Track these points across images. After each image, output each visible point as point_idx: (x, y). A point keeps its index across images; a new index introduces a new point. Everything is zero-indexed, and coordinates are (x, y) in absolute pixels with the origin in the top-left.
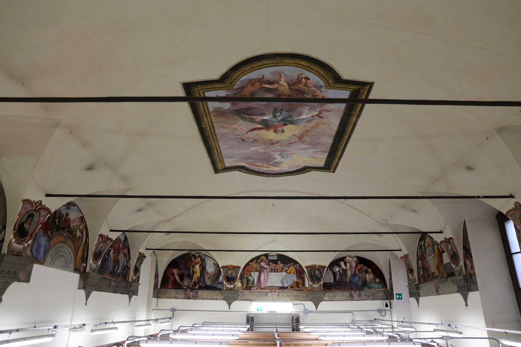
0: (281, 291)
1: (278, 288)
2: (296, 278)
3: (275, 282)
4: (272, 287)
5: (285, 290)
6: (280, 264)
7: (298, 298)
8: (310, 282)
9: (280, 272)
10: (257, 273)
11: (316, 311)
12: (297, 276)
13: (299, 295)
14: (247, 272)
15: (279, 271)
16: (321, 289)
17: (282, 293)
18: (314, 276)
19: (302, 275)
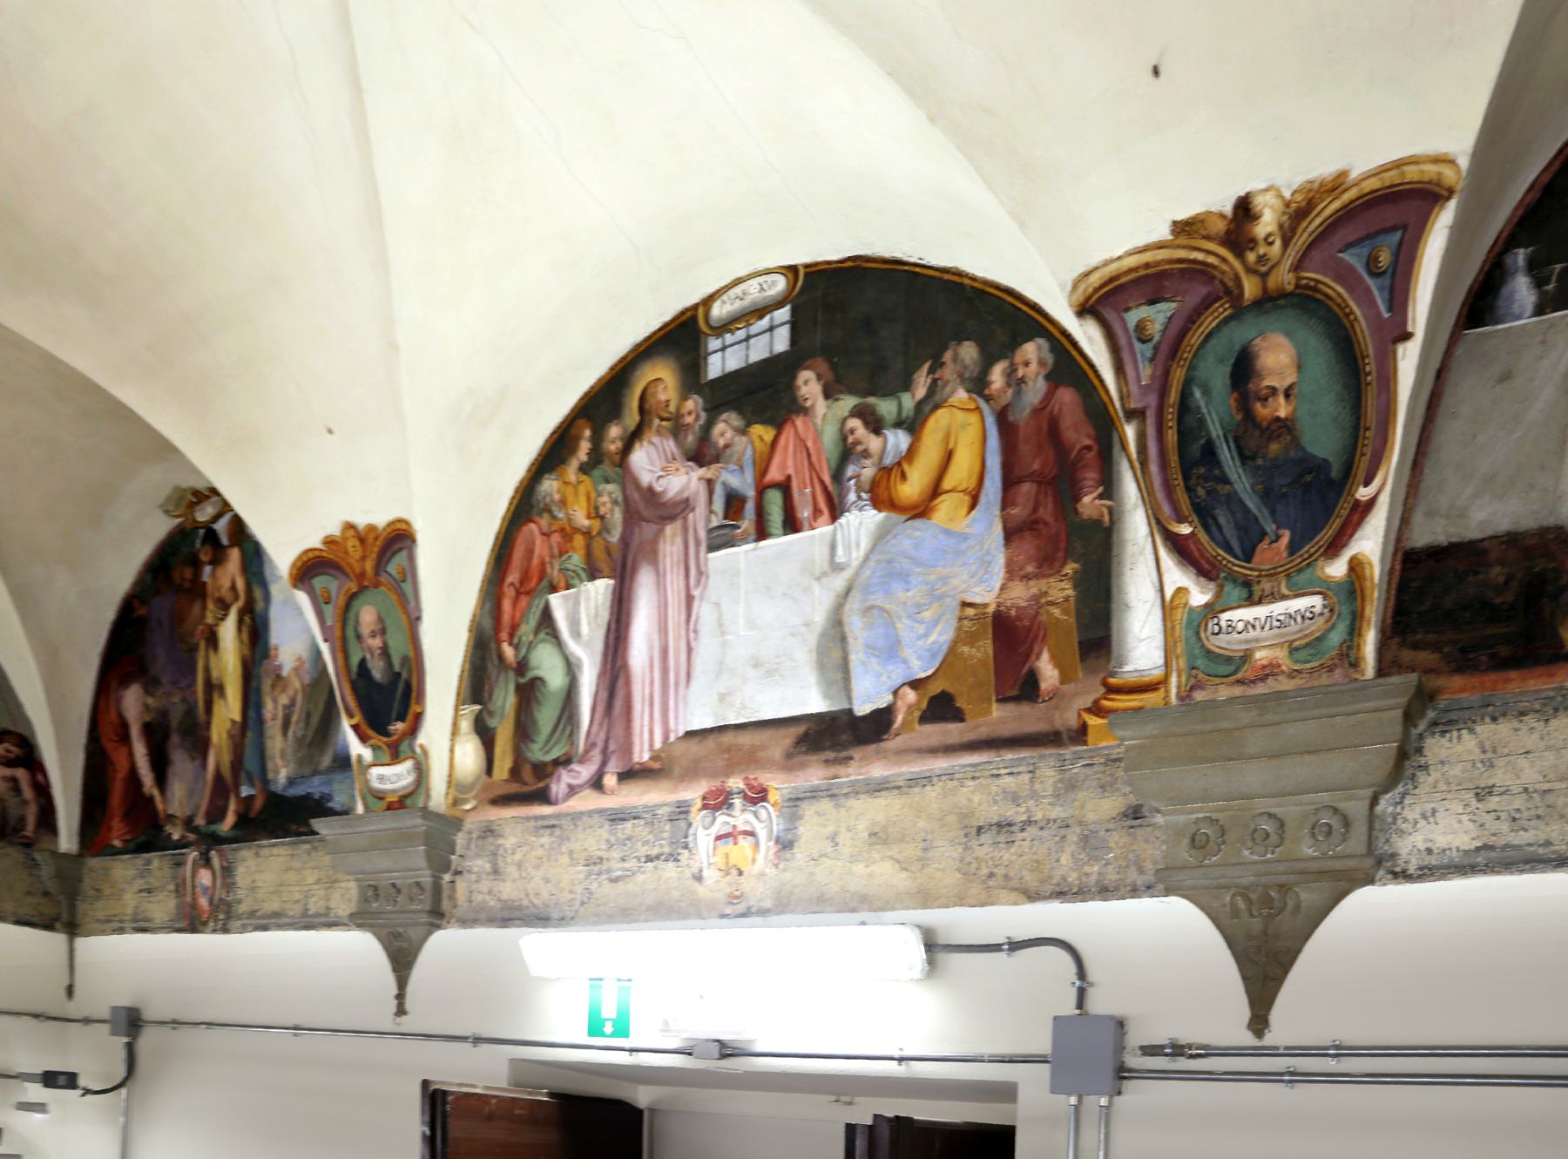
0: (814, 775)
1: (788, 737)
2: (1000, 560)
3: (757, 665)
4: (727, 738)
5: (856, 753)
6: (820, 406)
7: (1007, 855)
8: (1177, 576)
9: (817, 512)
10: (599, 590)
11: (1248, 1039)
12: (1010, 535)
13: (1016, 814)
14: (524, 600)
15: (805, 513)
16: (1355, 664)
17: (825, 805)
18: (1245, 457)
19: (1089, 503)
